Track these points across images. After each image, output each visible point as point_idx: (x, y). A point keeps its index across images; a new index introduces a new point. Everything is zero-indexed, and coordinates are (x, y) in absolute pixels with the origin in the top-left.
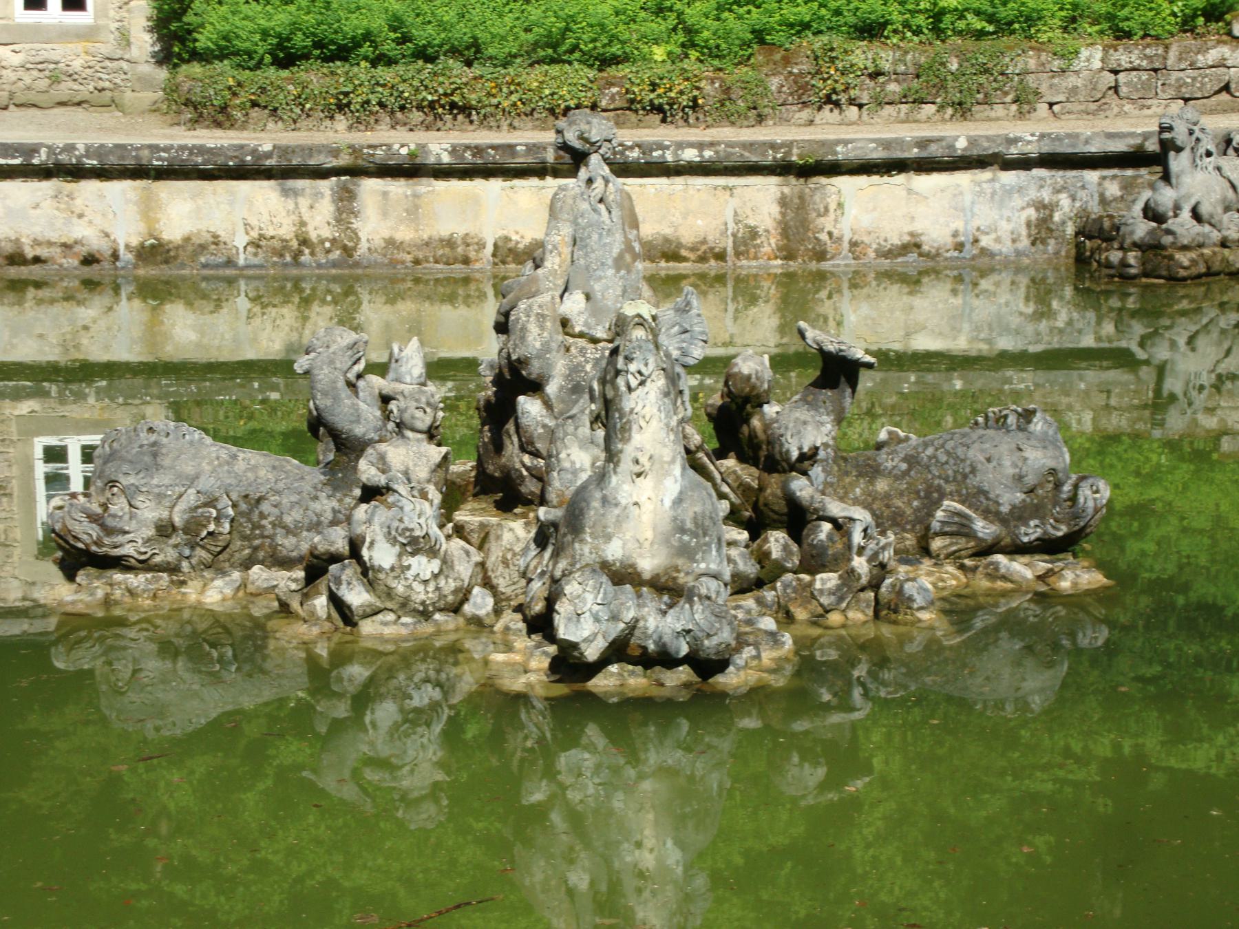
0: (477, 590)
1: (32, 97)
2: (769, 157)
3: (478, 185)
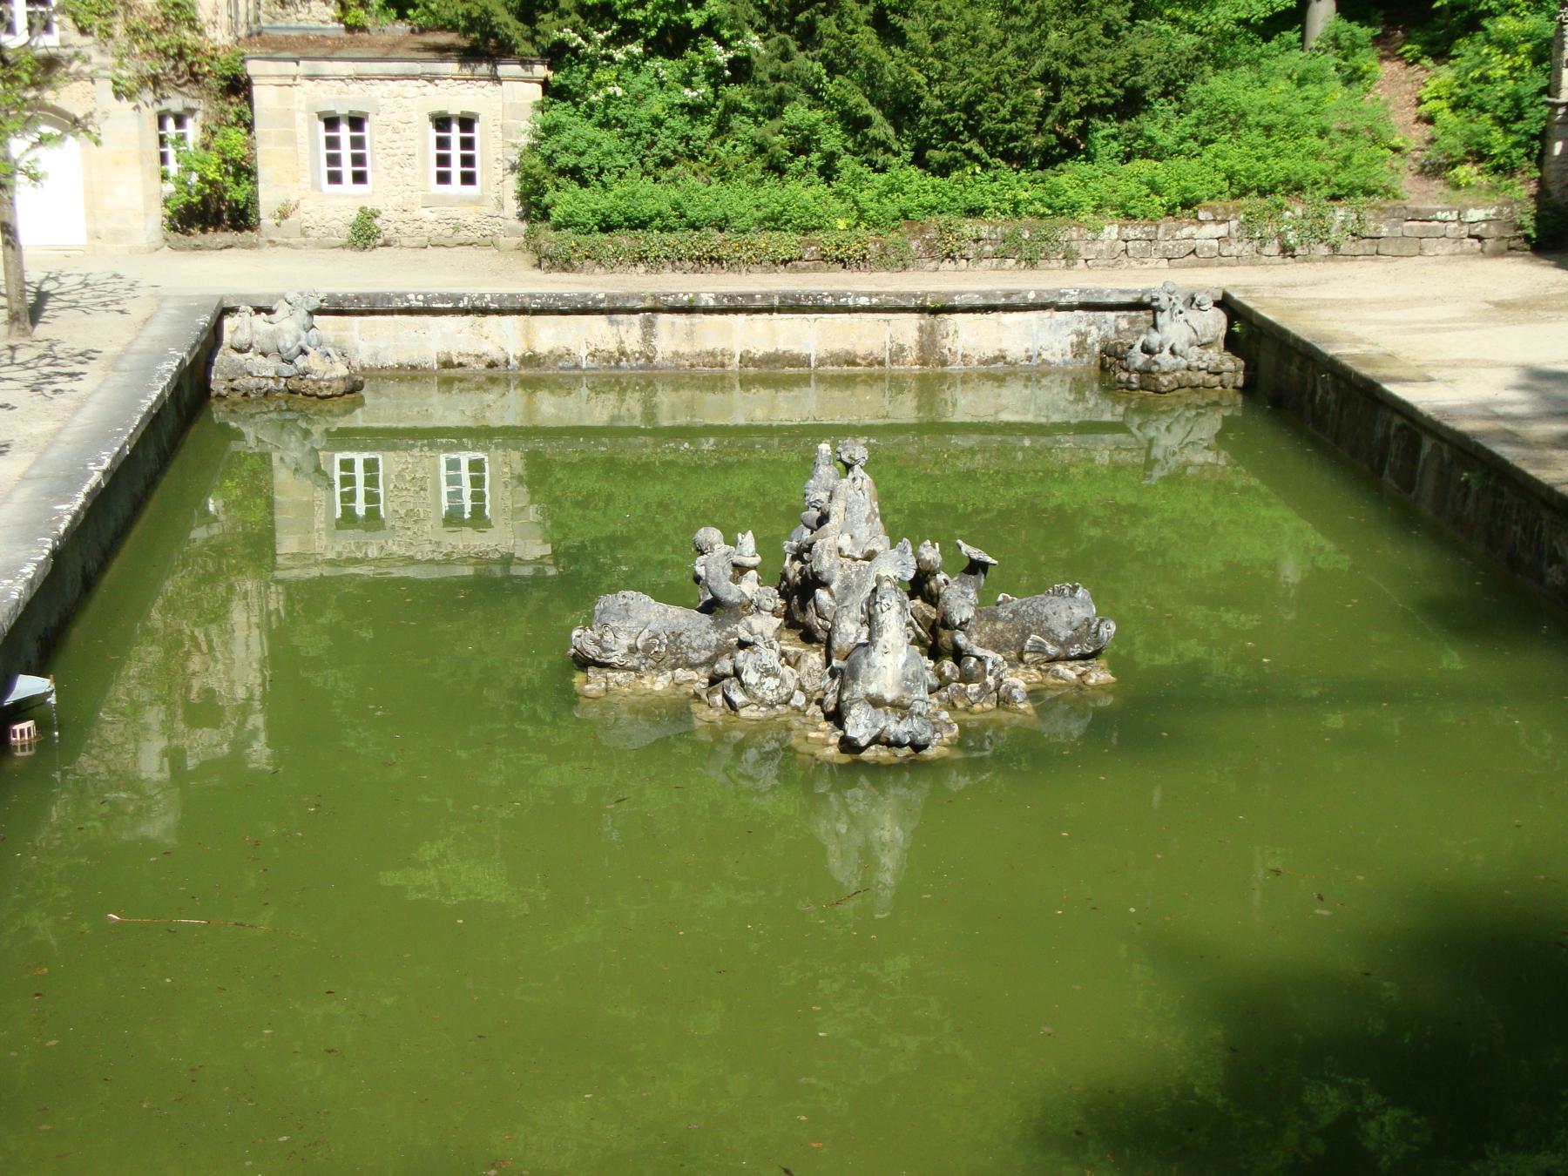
0: (797, 692)
1: (442, 240)
2: (913, 303)
3: (731, 317)
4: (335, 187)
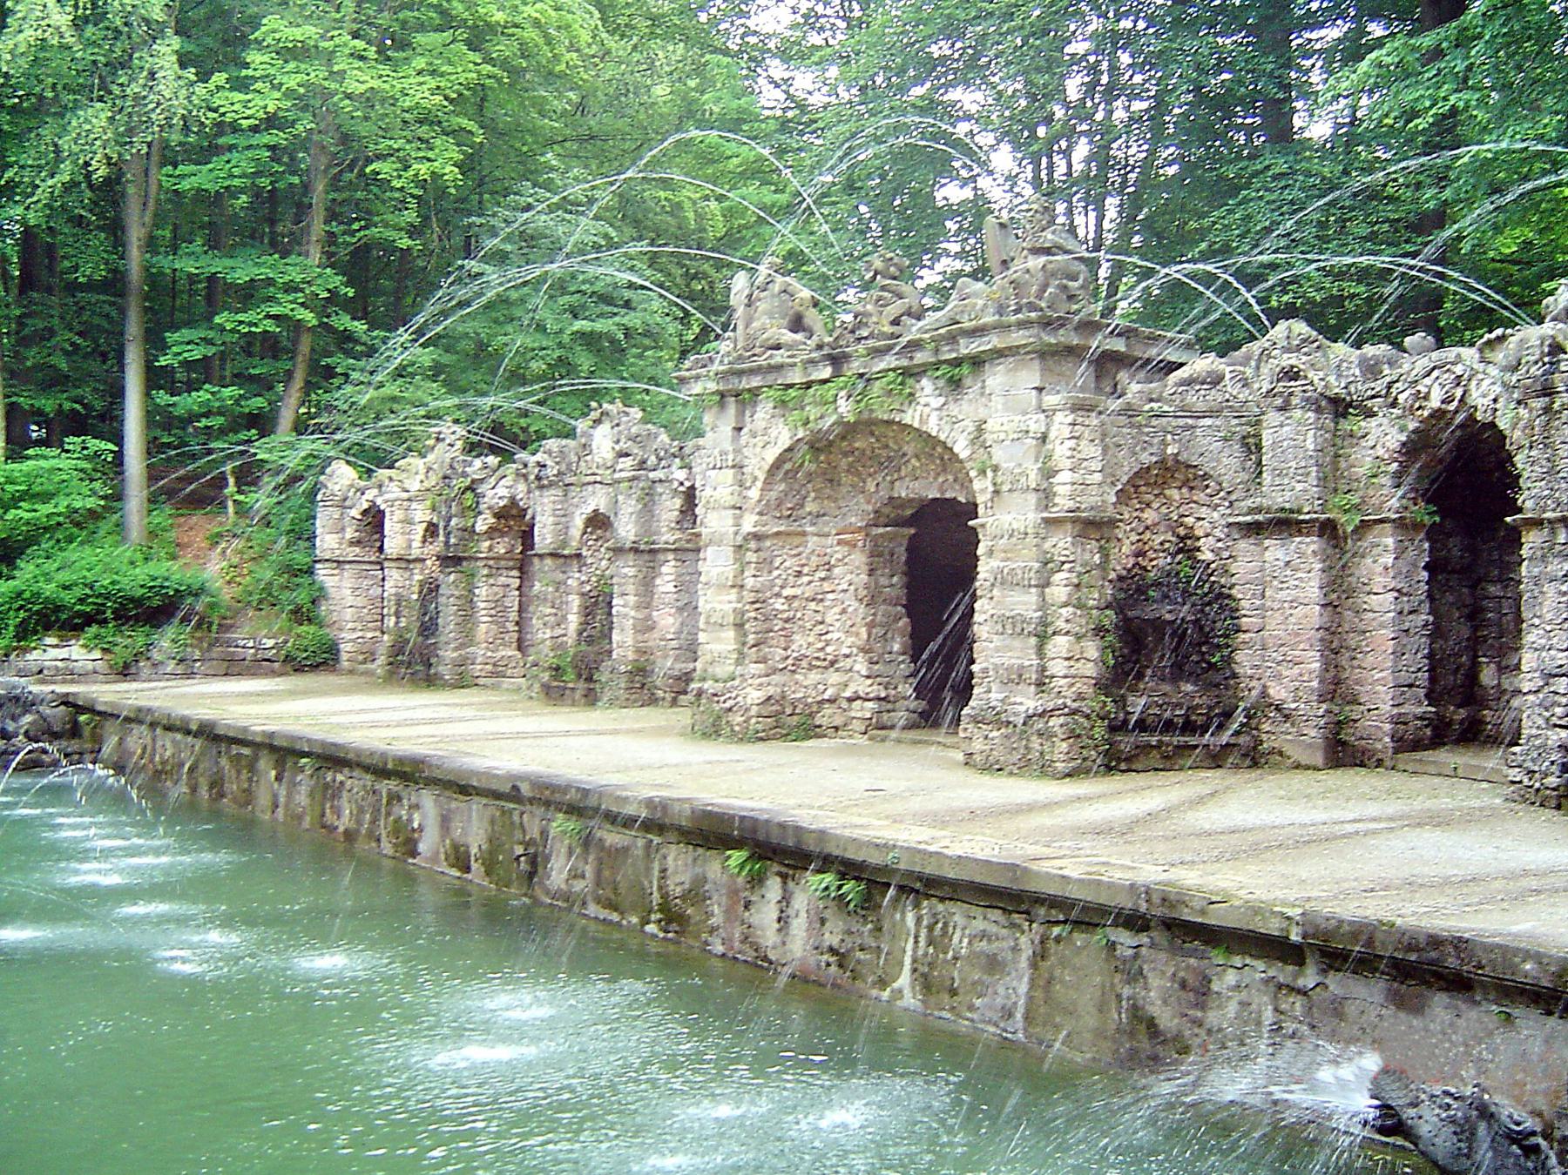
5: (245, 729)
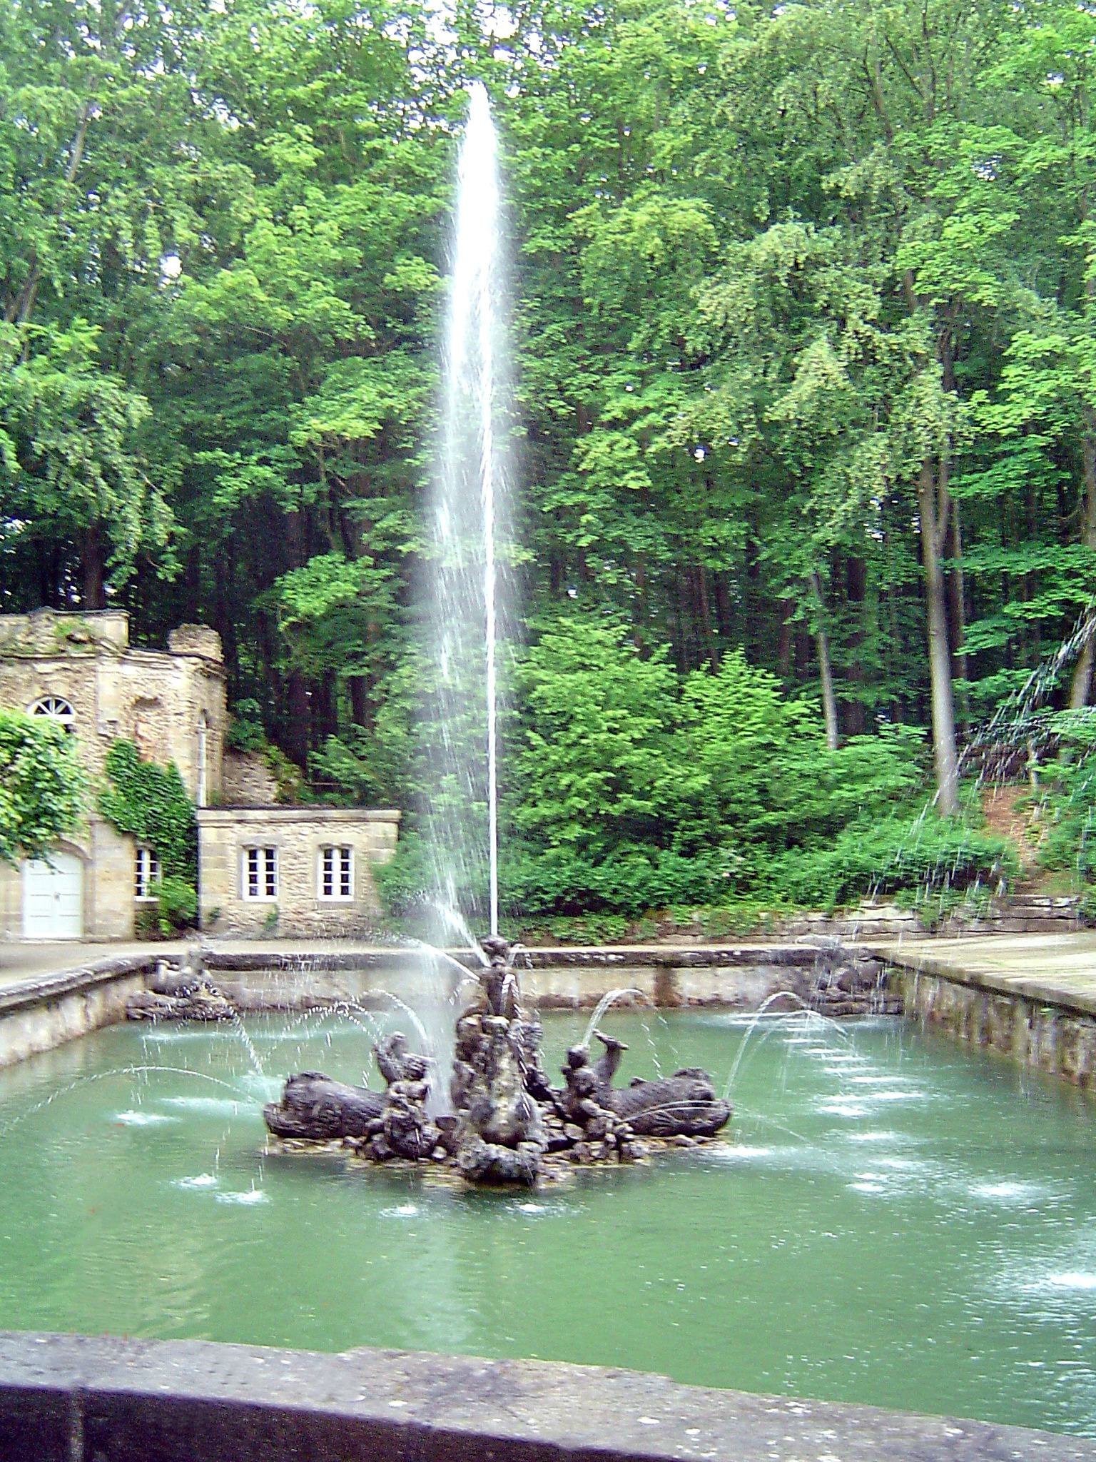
4: (253, 898)
5: (1003, 981)
